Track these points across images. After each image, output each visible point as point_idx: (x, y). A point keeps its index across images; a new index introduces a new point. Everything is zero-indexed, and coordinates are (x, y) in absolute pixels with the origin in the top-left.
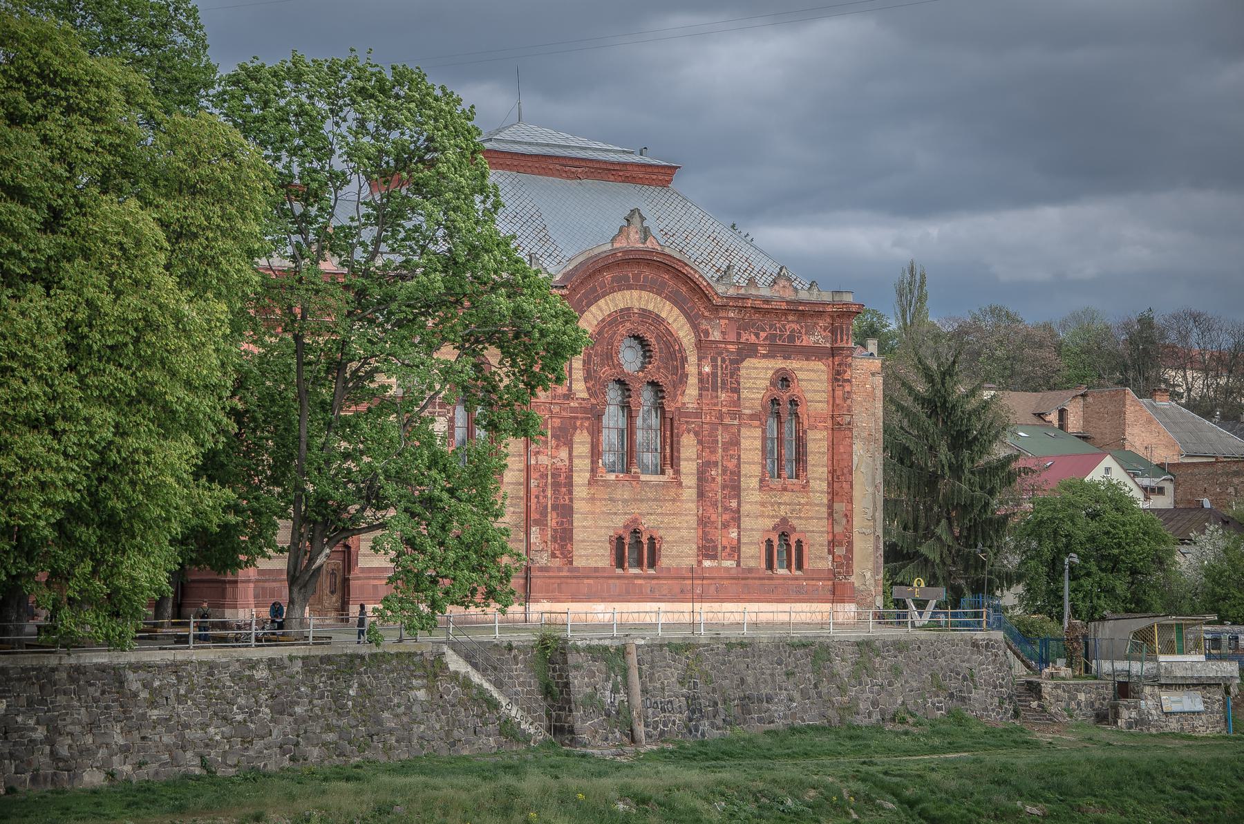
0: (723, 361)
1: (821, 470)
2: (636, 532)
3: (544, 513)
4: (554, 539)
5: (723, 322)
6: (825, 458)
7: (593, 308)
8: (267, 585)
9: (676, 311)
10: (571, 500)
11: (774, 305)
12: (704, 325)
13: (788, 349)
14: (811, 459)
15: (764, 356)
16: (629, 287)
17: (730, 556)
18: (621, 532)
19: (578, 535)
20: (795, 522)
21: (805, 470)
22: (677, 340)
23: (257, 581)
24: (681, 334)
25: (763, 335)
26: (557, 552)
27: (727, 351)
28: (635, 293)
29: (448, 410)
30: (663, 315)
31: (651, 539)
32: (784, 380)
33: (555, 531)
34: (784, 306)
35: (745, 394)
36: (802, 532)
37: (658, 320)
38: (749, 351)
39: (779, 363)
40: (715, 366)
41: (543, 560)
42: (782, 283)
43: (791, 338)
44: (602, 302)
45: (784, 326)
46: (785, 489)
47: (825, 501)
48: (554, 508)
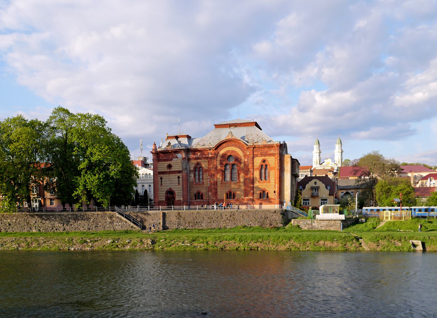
0: (250, 158)
1: (273, 178)
2: (230, 192)
3: (211, 189)
4: (214, 194)
5: (250, 151)
6: (274, 176)
7: (221, 151)
9: (239, 150)
10: (217, 187)
11: (260, 146)
12: (245, 152)
13: (266, 154)
14: (270, 176)
15: (260, 156)
16: (229, 146)
17: (251, 196)
18: (227, 192)
19: (218, 193)
20: (267, 189)
21: (269, 178)
22: (240, 155)
23: (158, 203)
24: (240, 154)
25: (259, 152)
26: (214, 197)
27: (251, 156)
28: (230, 147)
30: (236, 151)
31: (234, 193)
32: (264, 161)
33: (214, 192)
34: (263, 146)
35: (255, 164)
36: (269, 191)
37: (235, 152)
38: (257, 156)
39: (263, 158)
40: (248, 159)
41: (212, 198)
42: (264, 141)
43: (266, 152)
44: (223, 150)
45: (264, 150)
46: (264, 182)
47: (274, 184)
48: (214, 188)
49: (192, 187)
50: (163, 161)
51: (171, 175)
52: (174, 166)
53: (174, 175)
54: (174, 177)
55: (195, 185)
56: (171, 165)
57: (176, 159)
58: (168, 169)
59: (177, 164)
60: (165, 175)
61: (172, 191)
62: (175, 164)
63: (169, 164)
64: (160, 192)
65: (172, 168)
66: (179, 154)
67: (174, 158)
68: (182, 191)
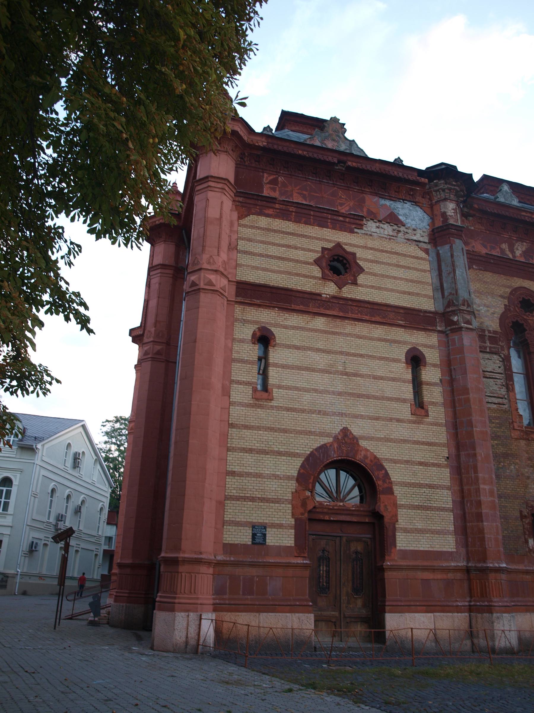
8: (238, 571)
29: (502, 347)
49: (506, 456)
50: (284, 215)
51: (349, 327)
52: (377, 269)
53: (379, 331)
54: (382, 349)
55: (523, 443)
56: (354, 254)
57: (388, 229)
58: (324, 278)
59: (394, 259)
60: (295, 319)
61: (359, 457)
62: (384, 258)
63: (339, 245)
64: (249, 458)
65: (361, 279)
66: (408, 205)
67: (373, 217)
68: (446, 473)
